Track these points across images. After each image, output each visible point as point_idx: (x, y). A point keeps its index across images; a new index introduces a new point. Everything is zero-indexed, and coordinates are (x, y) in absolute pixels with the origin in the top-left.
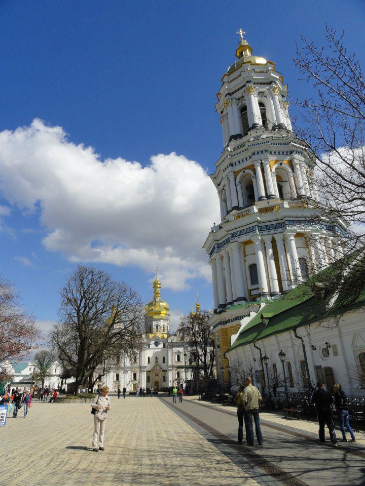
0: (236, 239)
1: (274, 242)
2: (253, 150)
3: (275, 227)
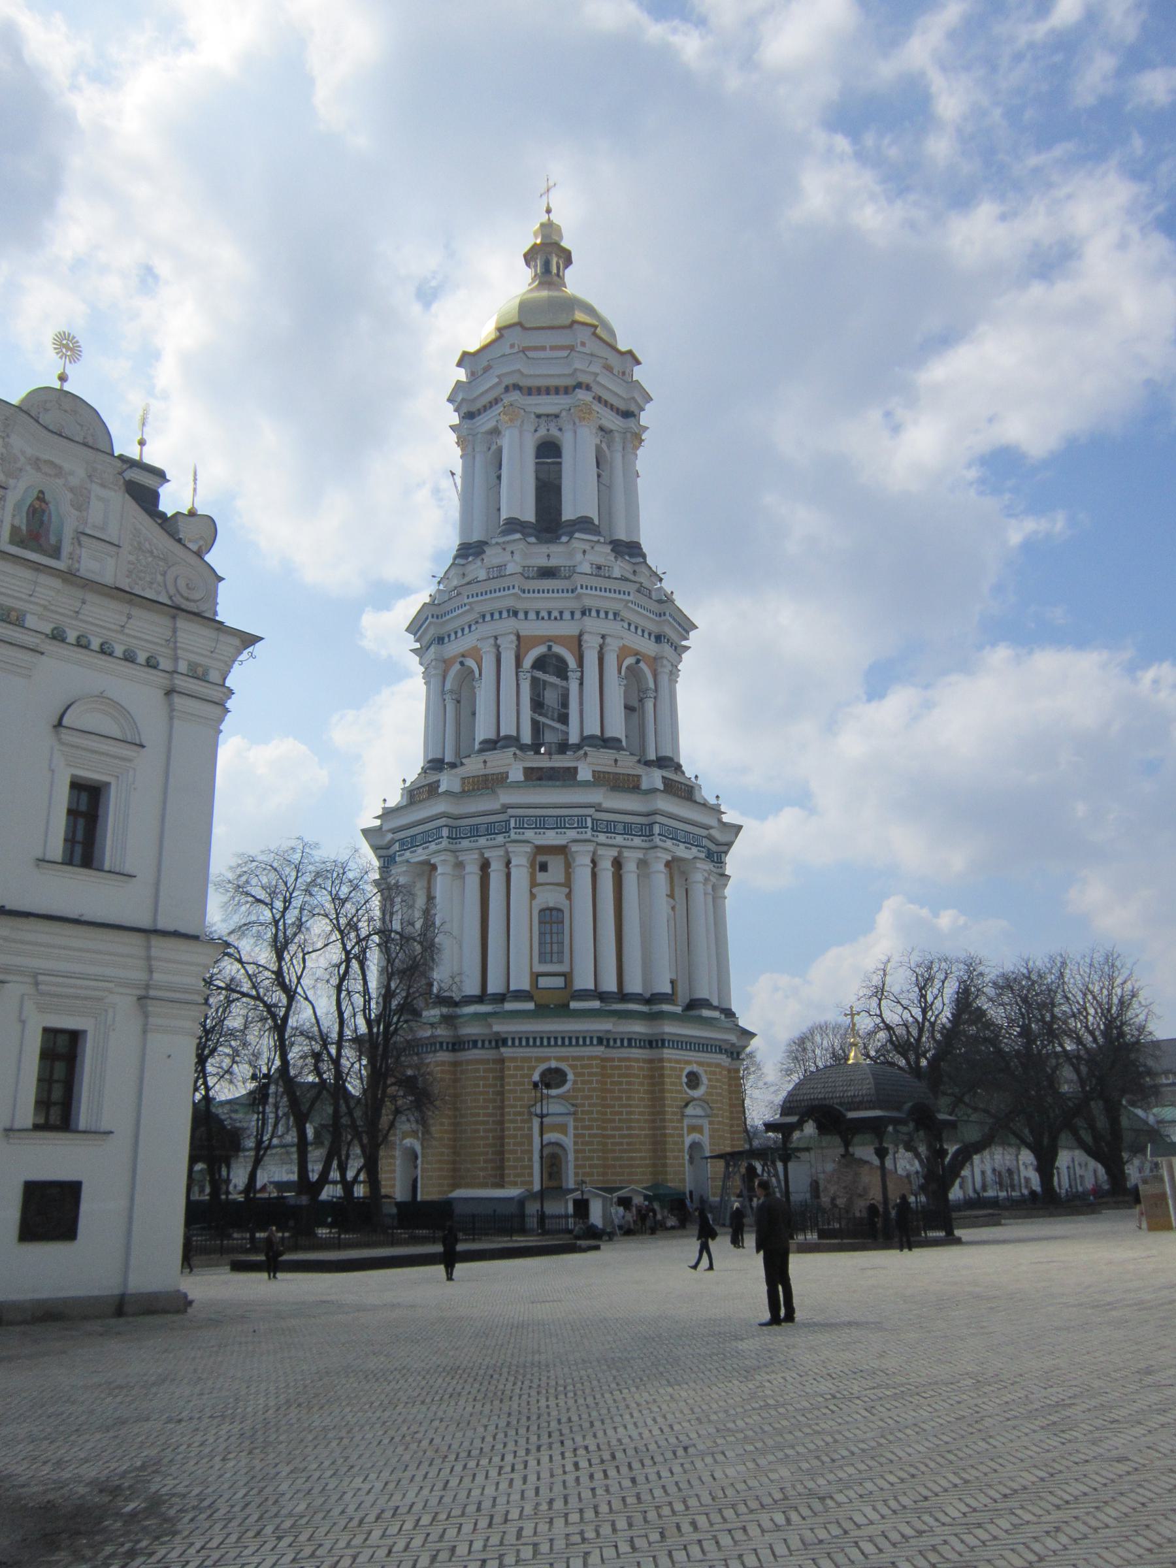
0: (408, 854)
1: (485, 866)
2: (479, 609)
3: (491, 830)
